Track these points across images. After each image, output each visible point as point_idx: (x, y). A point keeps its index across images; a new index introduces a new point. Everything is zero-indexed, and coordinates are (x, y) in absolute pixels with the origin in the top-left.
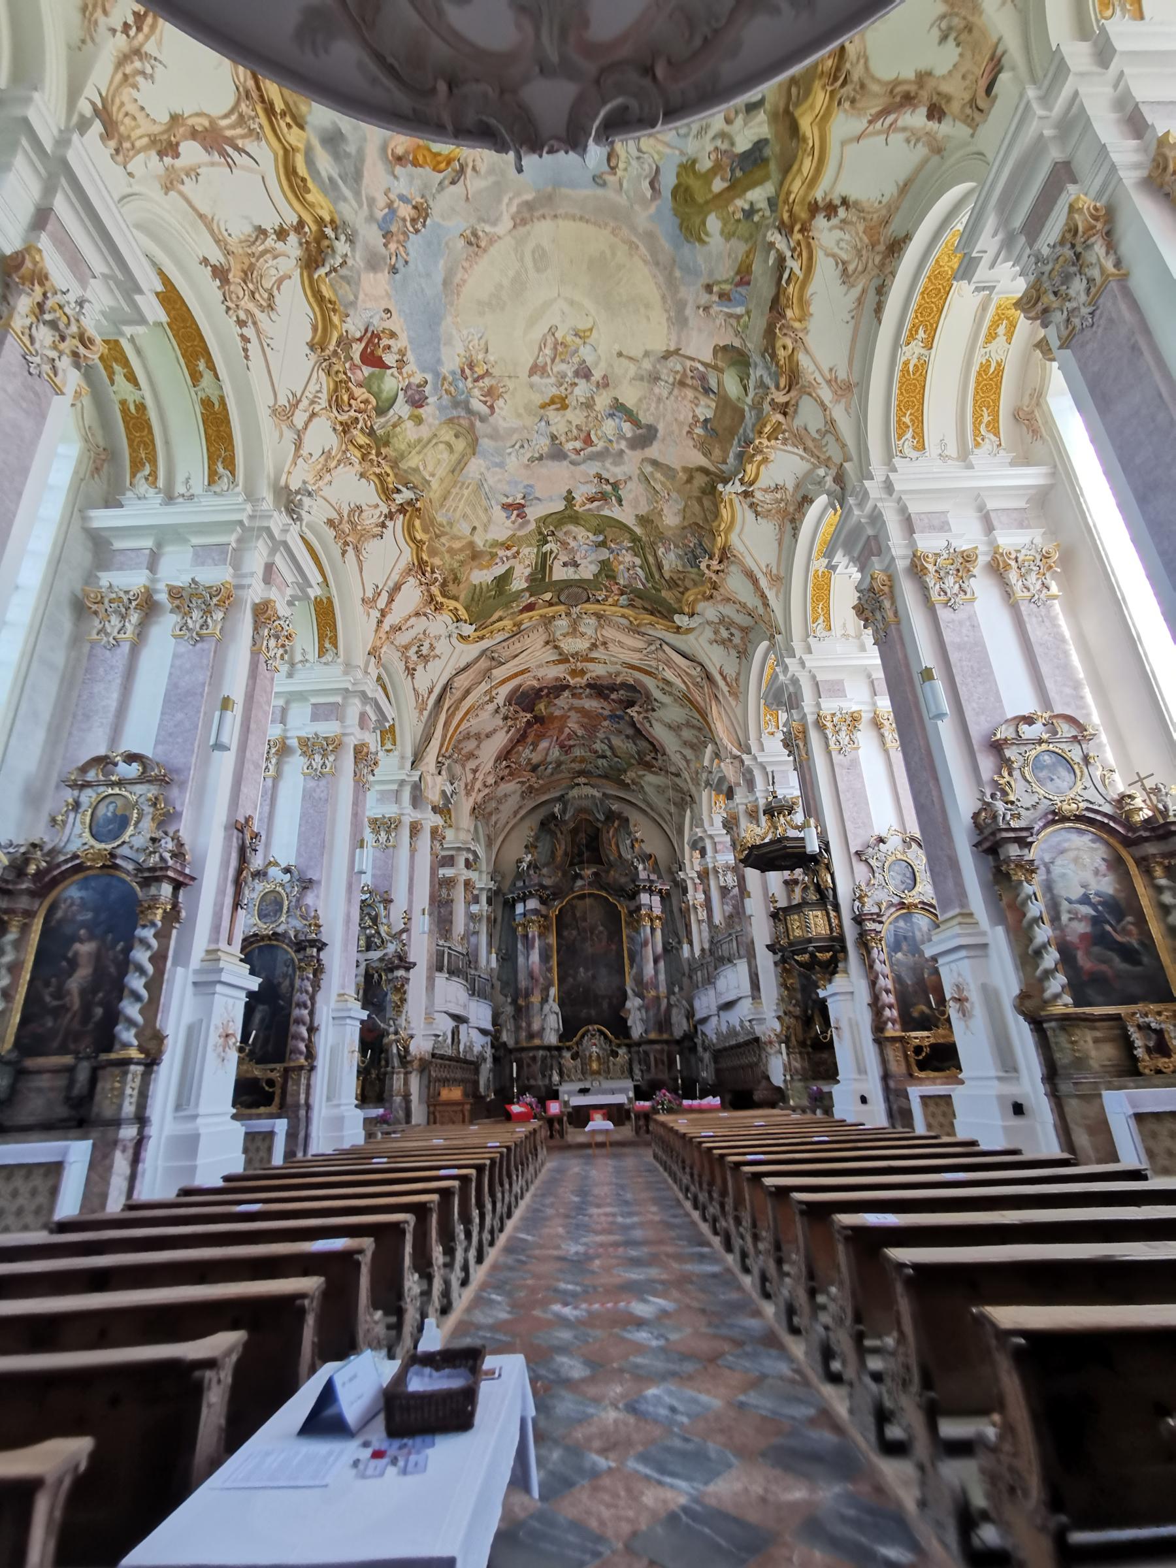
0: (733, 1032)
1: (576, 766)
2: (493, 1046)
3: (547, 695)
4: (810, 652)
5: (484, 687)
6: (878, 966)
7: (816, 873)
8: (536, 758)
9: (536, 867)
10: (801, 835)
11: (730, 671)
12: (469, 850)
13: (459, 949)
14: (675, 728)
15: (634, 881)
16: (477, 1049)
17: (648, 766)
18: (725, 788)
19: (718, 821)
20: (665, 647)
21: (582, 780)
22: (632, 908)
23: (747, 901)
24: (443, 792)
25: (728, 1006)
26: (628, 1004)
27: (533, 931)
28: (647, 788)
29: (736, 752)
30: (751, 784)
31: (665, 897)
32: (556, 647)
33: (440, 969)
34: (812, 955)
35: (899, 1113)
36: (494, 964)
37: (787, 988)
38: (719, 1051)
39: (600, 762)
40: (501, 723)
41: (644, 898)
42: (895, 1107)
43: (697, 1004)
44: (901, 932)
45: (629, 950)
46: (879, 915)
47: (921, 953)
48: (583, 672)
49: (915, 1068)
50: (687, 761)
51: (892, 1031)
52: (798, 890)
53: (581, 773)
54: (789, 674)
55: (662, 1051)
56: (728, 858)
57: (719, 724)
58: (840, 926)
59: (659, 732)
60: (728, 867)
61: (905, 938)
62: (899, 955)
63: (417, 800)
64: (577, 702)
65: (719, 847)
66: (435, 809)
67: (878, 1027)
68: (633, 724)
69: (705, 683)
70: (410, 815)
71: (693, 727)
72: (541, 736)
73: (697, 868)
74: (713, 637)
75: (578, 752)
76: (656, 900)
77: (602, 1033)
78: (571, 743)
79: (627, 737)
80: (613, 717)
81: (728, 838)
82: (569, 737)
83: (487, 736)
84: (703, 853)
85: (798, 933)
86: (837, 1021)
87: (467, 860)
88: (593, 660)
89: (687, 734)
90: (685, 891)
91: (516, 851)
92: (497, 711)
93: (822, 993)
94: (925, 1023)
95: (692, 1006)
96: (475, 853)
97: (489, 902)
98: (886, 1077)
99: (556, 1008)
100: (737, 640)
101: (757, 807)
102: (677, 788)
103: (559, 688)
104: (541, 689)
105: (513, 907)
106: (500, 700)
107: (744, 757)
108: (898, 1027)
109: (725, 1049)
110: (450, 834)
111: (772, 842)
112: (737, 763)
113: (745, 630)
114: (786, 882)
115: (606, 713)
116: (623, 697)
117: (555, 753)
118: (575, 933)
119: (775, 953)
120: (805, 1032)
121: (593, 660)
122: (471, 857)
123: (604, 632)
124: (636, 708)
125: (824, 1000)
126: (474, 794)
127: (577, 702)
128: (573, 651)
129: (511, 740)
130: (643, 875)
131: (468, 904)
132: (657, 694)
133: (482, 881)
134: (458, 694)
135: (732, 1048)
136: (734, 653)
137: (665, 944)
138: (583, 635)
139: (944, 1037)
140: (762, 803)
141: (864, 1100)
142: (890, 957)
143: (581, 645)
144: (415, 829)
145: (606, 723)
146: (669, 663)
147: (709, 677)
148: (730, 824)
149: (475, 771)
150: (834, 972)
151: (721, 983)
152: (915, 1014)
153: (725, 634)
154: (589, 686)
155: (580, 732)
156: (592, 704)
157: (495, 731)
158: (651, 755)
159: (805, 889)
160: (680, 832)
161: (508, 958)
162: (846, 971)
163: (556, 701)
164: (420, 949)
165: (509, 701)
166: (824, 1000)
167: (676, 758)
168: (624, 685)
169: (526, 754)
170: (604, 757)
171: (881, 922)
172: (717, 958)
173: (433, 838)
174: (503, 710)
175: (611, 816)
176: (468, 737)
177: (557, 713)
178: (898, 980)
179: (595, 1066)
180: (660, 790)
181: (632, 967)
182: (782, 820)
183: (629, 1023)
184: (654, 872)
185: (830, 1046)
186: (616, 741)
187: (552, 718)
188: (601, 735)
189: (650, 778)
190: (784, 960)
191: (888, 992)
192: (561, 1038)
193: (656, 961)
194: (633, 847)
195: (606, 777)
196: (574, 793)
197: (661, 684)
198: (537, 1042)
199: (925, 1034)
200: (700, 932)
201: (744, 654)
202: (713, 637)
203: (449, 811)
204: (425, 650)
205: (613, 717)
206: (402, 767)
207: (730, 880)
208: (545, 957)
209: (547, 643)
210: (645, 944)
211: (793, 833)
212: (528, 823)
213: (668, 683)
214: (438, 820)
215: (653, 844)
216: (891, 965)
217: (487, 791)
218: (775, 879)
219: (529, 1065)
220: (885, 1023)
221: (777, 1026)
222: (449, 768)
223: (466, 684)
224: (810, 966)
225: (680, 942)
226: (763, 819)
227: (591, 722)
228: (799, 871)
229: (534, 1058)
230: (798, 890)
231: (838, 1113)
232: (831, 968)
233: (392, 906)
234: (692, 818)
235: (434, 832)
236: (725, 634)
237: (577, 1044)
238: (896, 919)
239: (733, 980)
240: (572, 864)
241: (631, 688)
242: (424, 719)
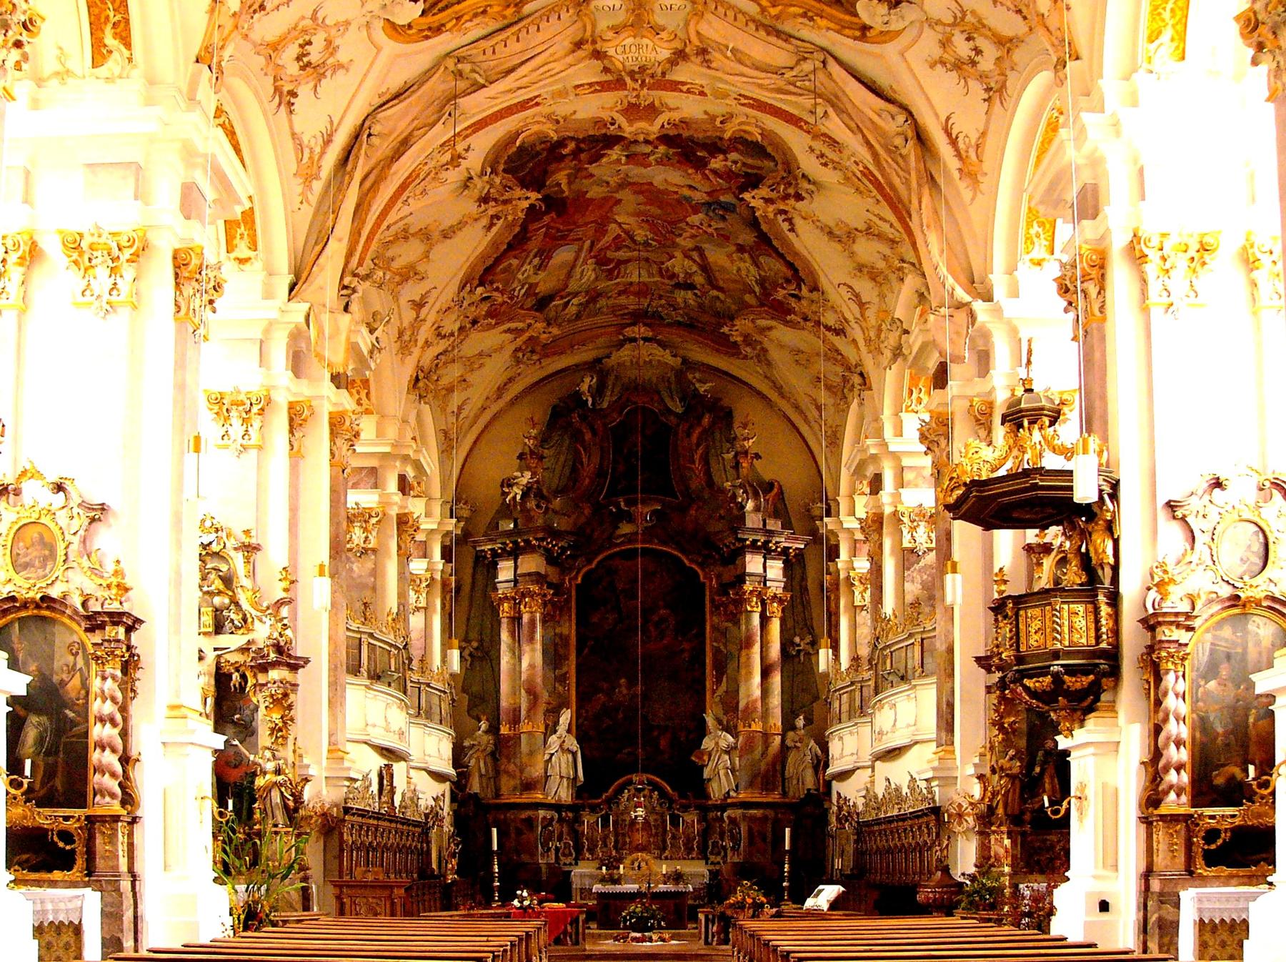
0: (895, 795)
1: (630, 302)
2: (453, 799)
3: (576, 154)
4: (1135, 104)
5: (441, 133)
6: (1171, 702)
7: (1085, 535)
8: (545, 282)
9: (540, 495)
10: (1067, 466)
11: (967, 127)
12: (406, 458)
13: (390, 638)
14: (842, 236)
15: (734, 531)
16: (426, 802)
17: (781, 311)
18: (932, 364)
19: (912, 424)
20: (833, 67)
21: (640, 331)
22: (727, 578)
23: (949, 578)
24: (353, 348)
25: (893, 753)
26: (707, 743)
27: (531, 612)
28: (774, 354)
29: (962, 295)
30: (984, 360)
31: (793, 564)
32: (598, 55)
33: (354, 670)
34: (1057, 678)
35: (1159, 927)
36: (456, 666)
37: (1002, 729)
38: (867, 824)
39: (681, 296)
40: (471, 207)
41: (754, 564)
42: (1153, 918)
43: (834, 748)
44: (1223, 647)
45: (717, 652)
46: (1188, 616)
47: (1252, 685)
48: (652, 111)
49: (1199, 862)
50: (862, 305)
51: (1174, 804)
52: (1048, 562)
53: (638, 317)
54: (1087, 148)
55: (765, 818)
56: (922, 496)
57: (933, 238)
58: (1116, 632)
59: (808, 242)
60: (920, 513)
61: (1228, 657)
62: (1212, 685)
63: (297, 364)
64: (636, 173)
65: (908, 476)
66: (338, 380)
67: (1152, 800)
68: (754, 223)
69: (910, 149)
70: (286, 388)
71: (880, 236)
72: (556, 239)
73: (861, 512)
74: (937, 52)
75: (635, 275)
76: (775, 570)
77: (655, 786)
78: (622, 254)
79: (741, 249)
80: (713, 206)
81: (927, 461)
82: (617, 243)
83: (446, 235)
84: (876, 485)
85: (1035, 640)
86: (1083, 787)
87: (402, 479)
88: (675, 86)
89: (867, 250)
90: (834, 553)
91: (506, 469)
92: (467, 182)
93: (1063, 742)
94: (1235, 793)
95: (825, 748)
96: (418, 466)
97: (446, 554)
98: (1148, 874)
99: (572, 743)
100: (987, 63)
101: (991, 405)
102: (835, 355)
103: (599, 142)
104: (562, 143)
105: (492, 569)
106: (474, 161)
107: (979, 306)
108: (1184, 798)
109: (878, 822)
110: (368, 427)
111: (1010, 477)
112: (961, 316)
113: (1006, 44)
114: (1029, 549)
115: (699, 197)
116: (741, 171)
117: (587, 274)
118: (611, 617)
119: (989, 671)
120: (1023, 801)
121: (675, 86)
122: (410, 473)
123: (704, 28)
124: (764, 191)
125: (1066, 753)
126: (416, 352)
127: (636, 173)
128: (632, 65)
129: (494, 244)
130: (753, 520)
131: (404, 557)
132: (808, 163)
133: (432, 519)
134: (382, 147)
135: (889, 820)
136: (977, 88)
137: (786, 644)
138: (657, 30)
139: (1259, 816)
140: (1001, 398)
141: (1104, 906)
142: (1195, 686)
143: (656, 52)
144: (297, 418)
145: (695, 219)
146: (836, 103)
147: (921, 138)
148: (936, 434)
149: (418, 305)
150: (1091, 709)
151: (884, 718)
152: (1219, 781)
153: (963, 48)
154: (665, 139)
155: (641, 234)
156: (669, 178)
157: (461, 224)
158: (786, 287)
159: (1063, 562)
160: (835, 441)
161: (481, 657)
162: (1112, 708)
163: (593, 168)
164: (316, 633)
165: (492, 163)
166: (1066, 753)
167: (839, 297)
168: (743, 143)
169: (525, 272)
170: (690, 286)
171: (1190, 629)
172: (882, 674)
173: (334, 434)
174: (480, 185)
175: (696, 404)
176: (405, 235)
177: (595, 192)
178: (1202, 725)
179: (640, 838)
180: (801, 358)
181: (719, 682)
182: (1036, 432)
183: (706, 773)
184: (776, 515)
185: (1064, 824)
186: (718, 256)
187: (581, 202)
188: (685, 242)
189: (782, 334)
190: (1002, 684)
191: (1178, 743)
192: (580, 791)
193: (766, 673)
194: (737, 466)
195: (690, 326)
196: (625, 354)
197: (819, 146)
198: (539, 796)
199: (1229, 811)
200: (854, 626)
201: (996, 92)
202: (937, 52)
203: (366, 382)
204: (315, 54)
205: (713, 206)
206: (268, 295)
207: (923, 537)
208: (554, 656)
209: (578, 45)
210: (748, 644)
211: (1052, 462)
212: (524, 411)
213: (833, 143)
214: (345, 400)
215: (778, 462)
216: (1195, 702)
217: (443, 345)
218: (1007, 543)
219: (519, 832)
220: (1166, 793)
221: (976, 790)
222: (365, 301)
223: (402, 127)
224: (1047, 697)
225: (814, 644)
226: (1000, 432)
227: (666, 212)
228: (1054, 530)
229: (530, 823)
230: (1048, 562)
231: (1058, 927)
232: (1086, 702)
233: (258, 557)
234: (861, 419)
235: (337, 424)
236: (963, 48)
237: (609, 801)
238: (1219, 624)
239: (909, 712)
240: (613, 493)
241: (756, 149)
242: (314, 199)
